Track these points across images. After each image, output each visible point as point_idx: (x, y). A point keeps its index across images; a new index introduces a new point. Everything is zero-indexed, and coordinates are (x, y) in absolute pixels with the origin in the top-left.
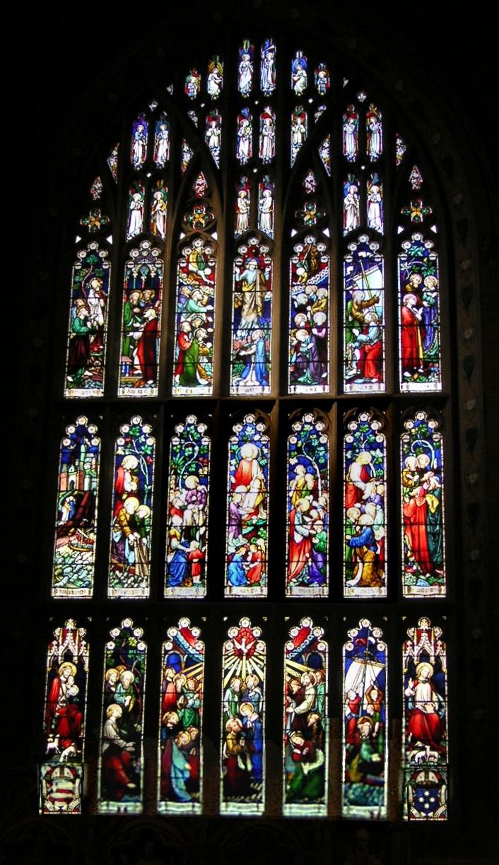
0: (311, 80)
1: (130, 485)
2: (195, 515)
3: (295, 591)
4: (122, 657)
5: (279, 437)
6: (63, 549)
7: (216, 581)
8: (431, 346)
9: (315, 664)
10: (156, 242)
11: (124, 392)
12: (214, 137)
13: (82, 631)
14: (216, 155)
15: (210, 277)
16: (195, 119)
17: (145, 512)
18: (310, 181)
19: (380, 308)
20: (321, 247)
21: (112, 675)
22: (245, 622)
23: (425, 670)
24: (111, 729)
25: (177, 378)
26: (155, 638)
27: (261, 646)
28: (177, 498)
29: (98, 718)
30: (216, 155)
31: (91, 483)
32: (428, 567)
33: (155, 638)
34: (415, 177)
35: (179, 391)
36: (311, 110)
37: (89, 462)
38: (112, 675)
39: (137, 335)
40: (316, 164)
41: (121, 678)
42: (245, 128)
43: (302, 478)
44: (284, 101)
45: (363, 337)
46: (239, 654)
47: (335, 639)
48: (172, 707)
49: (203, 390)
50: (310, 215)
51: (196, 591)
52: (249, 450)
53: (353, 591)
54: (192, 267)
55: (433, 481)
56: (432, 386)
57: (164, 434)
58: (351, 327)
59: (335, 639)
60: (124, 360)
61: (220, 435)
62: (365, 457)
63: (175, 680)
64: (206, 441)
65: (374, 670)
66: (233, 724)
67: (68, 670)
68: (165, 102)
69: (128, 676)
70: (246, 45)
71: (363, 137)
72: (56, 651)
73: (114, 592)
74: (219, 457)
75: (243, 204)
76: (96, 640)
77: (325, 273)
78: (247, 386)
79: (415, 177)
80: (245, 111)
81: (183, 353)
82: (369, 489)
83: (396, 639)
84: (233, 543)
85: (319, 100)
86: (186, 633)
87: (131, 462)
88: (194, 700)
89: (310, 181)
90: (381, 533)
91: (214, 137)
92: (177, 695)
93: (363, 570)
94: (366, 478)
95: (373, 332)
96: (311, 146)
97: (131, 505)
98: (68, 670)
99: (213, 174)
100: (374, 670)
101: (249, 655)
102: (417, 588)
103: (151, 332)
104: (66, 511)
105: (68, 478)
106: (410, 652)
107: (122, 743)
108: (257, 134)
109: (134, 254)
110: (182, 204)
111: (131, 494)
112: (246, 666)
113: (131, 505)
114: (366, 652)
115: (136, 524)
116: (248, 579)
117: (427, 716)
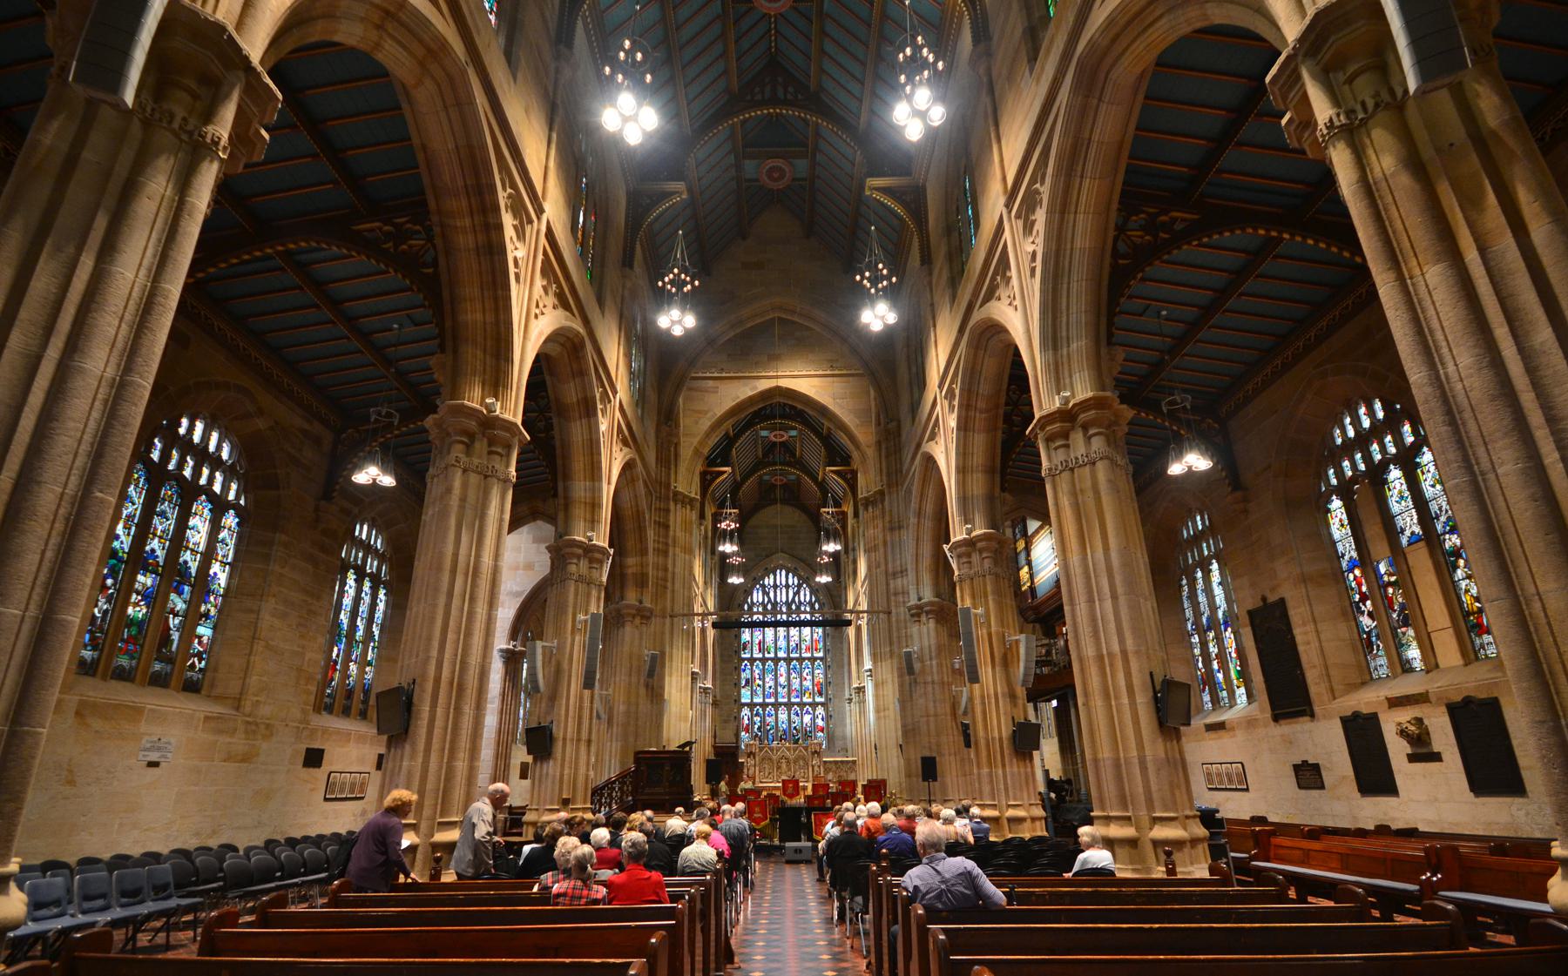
1: (757, 677)
2: (772, 683)
3: (793, 700)
4: (757, 714)
6: (743, 691)
7: (776, 699)
8: (820, 645)
9: (798, 715)
11: (755, 656)
12: (772, 595)
17: (761, 683)
18: (794, 607)
21: (755, 718)
23: (820, 717)
26: (764, 710)
28: (767, 680)
29: (753, 728)
31: (749, 676)
32: (820, 694)
33: (764, 710)
34: (817, 606)
35: (767, 655)
37: (748, 671)
38: (755, 718)
41: (757, 719)
43: (794, 675)
44: (787, 586)
47: (802, 710)
49: (772, 655)
51: (772, 700)
52: (782, 669)
53: (805, 700)
55: (821, 676)
56: (821, 654)
57: (764, 665)
59: (802, 710)
61: (776, 665)
62: (807, 671)
63: (768, 720)
65: (810, 716)
67: (746, 718)
68: (761, 586)
69: (759, 719)
71: (805, 595)
72: (743, 714)
73: (755, 701)
74: (776, 670)
76: (751, 711)
78: (781, 654)
79: (817, 606)
83: (814, 710)
84: (780, 689)
87: (757, 671)
89: (794, 607)
90: (811, 687)
91: (772, 595)
93: (807, 695)
97: (758, 682)
98: (746, 718)
99: (772, 604)
100: (810, 716)
102: (818, 699)
104: (743, 683)
105: (743, 675)
106: (817, 713)
113: (758, 682)
114: (808, 712)
115: (759, 685)
116: (783, 697)
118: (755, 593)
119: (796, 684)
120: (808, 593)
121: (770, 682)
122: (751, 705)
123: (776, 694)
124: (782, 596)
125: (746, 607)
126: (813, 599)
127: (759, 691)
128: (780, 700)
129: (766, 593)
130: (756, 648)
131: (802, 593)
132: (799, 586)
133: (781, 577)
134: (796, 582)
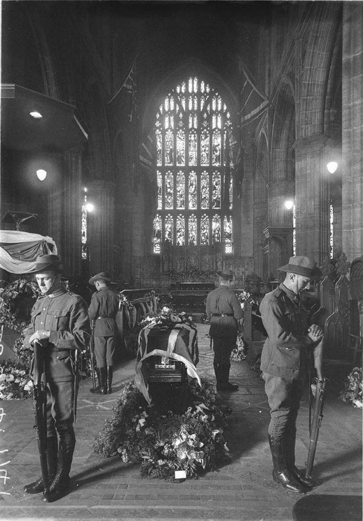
0: (205, 89)
5: (199, 175)
7: (187, 206)
10: (172, 130)
13: (160, 217)
14: (184, 109)
15: (184, 139)
16: (179, 99)
18: (205, 115)
19: (220, 146)
20: (207, 132)
22: (193, 215)
24: (167, 236)
25: (177, 162)
27: (196, 220)
28: (178, 189)
30: (184, 109)
34: (228, 115)
35: (178, 165)
36: (205, 97)
39: (168, 152)
40: (207, 112)
42: (190, 102)
45: (216, 154)
46: (192, 221)
48: (178, 231)
49: (183, 165)
50: (205, 124)
54: (180, 136)
57: (175, 175)
58: (214, 151)
60: (166, 158)
63: (179, 226)
64: (184, 176)
66: (191, 235)
67: (157, 224)
70: (190, 81)
71: (217, 103)
73: (167, 208)
75: (190, 121)
77: (209, 138)
79: (228, 115)
80: (190, 97)
81: (178, 156)
82: (217, 187)
85: (207, 94)
86: (181, 217)
88: (183, 230)
89: (205, 115)
91: (183, 103)
92: (180, 229)
94: (216, 184)
95: (218, 152)
96: (205, 107)
99: (184, 113)
101: (194, 221)
103: (171, 150)
107: (169, 239)
108: (193, 103)
109: (167, 133)
110: (177, 120)
111: (169, 188)
112: (193, 224)
114: (217, 221)
117: (228, 233)
118: (167, 101)
119: (205, 194)
120: (220, 102)
121: (181, 187)
122: (163, 213)
123: (186, 202)
124: (192, 105)
125: (158, 116)
126: (225, 108)
127: (170, 200)
128: (191, 207)
129: (177, 102)
130: (167, 159)
131: (214, 102)
132: (212, 94)
133: (193, 85)
134: (208, 90)
